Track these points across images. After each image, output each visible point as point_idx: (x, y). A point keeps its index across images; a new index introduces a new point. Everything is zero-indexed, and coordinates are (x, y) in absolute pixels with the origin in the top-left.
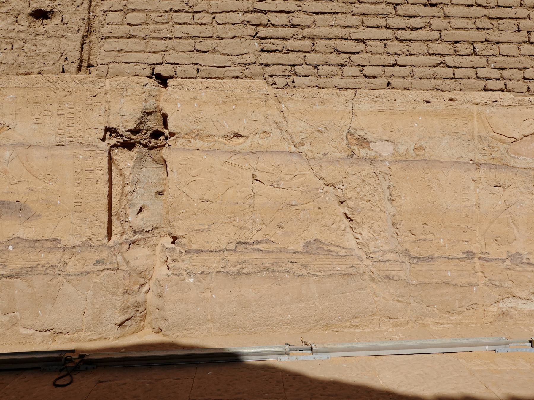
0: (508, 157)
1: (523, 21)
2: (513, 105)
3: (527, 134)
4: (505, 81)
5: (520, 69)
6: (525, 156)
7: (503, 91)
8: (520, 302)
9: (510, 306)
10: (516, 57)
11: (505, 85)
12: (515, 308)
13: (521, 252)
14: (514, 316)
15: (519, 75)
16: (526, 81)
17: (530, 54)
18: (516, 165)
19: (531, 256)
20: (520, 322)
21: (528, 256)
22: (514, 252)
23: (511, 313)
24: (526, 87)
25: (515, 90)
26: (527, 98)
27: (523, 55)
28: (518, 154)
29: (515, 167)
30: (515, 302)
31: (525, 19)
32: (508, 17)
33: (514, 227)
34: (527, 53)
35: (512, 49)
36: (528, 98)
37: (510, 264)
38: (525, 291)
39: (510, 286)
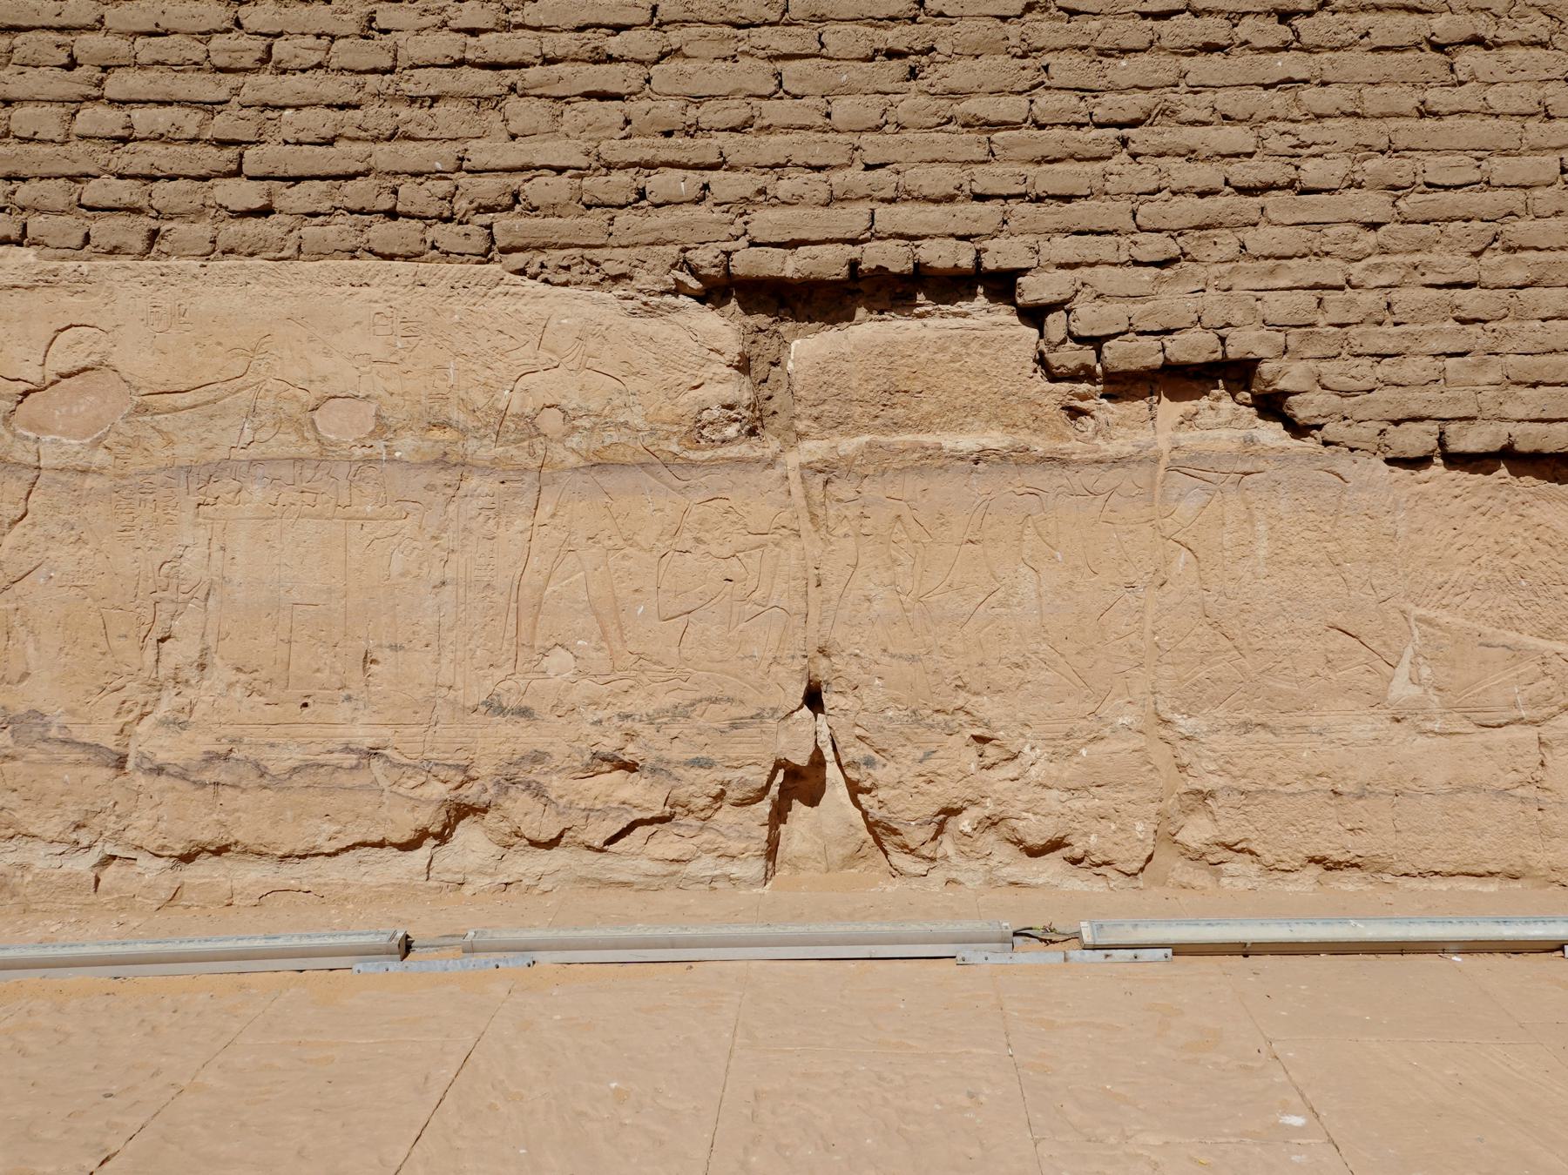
0: (8, 437)
1: (87, 36)
2: (25, 284)
3: (65, 370)
4: (25, 215)
5: (71, 178)
6: (62, 433)
7: (20, 244)
8: (40, 849)
9: (10, 861)
10: (63, 143)
11: (25, 225)
12: (24, 867)
13: (45, 709)
14: (22, 891)
15: (55, 193)
16: (90, 214)
17: (101, 133)
18: (30, 459)
19: (76, 720)
20: (40, 907)
21: (64, 719)
22: (22, 709)
23: (16, 880)
24: (80, 234)
25: (47, 241)
26: (70, 265)
27: (83, 138)
28: (42, 429)
29: (26, 467)
30: (31, 850)
31: (92, 29)
32: (38, 24)
33: (31, 638)
34: (91, 132)
35: (48, 120)
36: (74, 264)
37: (10, 742)
38: (55, 820)
39: (12, 805)
